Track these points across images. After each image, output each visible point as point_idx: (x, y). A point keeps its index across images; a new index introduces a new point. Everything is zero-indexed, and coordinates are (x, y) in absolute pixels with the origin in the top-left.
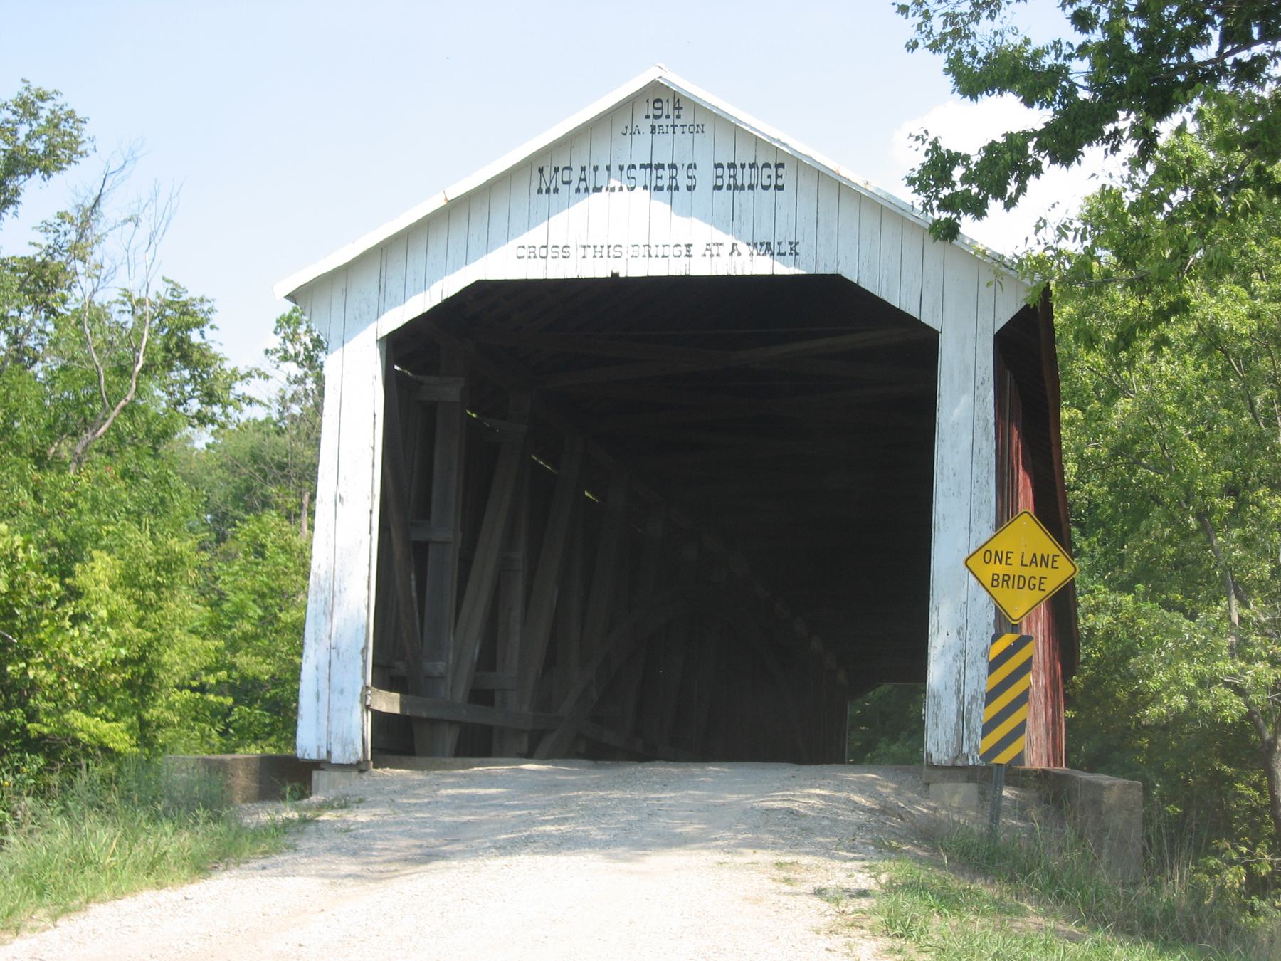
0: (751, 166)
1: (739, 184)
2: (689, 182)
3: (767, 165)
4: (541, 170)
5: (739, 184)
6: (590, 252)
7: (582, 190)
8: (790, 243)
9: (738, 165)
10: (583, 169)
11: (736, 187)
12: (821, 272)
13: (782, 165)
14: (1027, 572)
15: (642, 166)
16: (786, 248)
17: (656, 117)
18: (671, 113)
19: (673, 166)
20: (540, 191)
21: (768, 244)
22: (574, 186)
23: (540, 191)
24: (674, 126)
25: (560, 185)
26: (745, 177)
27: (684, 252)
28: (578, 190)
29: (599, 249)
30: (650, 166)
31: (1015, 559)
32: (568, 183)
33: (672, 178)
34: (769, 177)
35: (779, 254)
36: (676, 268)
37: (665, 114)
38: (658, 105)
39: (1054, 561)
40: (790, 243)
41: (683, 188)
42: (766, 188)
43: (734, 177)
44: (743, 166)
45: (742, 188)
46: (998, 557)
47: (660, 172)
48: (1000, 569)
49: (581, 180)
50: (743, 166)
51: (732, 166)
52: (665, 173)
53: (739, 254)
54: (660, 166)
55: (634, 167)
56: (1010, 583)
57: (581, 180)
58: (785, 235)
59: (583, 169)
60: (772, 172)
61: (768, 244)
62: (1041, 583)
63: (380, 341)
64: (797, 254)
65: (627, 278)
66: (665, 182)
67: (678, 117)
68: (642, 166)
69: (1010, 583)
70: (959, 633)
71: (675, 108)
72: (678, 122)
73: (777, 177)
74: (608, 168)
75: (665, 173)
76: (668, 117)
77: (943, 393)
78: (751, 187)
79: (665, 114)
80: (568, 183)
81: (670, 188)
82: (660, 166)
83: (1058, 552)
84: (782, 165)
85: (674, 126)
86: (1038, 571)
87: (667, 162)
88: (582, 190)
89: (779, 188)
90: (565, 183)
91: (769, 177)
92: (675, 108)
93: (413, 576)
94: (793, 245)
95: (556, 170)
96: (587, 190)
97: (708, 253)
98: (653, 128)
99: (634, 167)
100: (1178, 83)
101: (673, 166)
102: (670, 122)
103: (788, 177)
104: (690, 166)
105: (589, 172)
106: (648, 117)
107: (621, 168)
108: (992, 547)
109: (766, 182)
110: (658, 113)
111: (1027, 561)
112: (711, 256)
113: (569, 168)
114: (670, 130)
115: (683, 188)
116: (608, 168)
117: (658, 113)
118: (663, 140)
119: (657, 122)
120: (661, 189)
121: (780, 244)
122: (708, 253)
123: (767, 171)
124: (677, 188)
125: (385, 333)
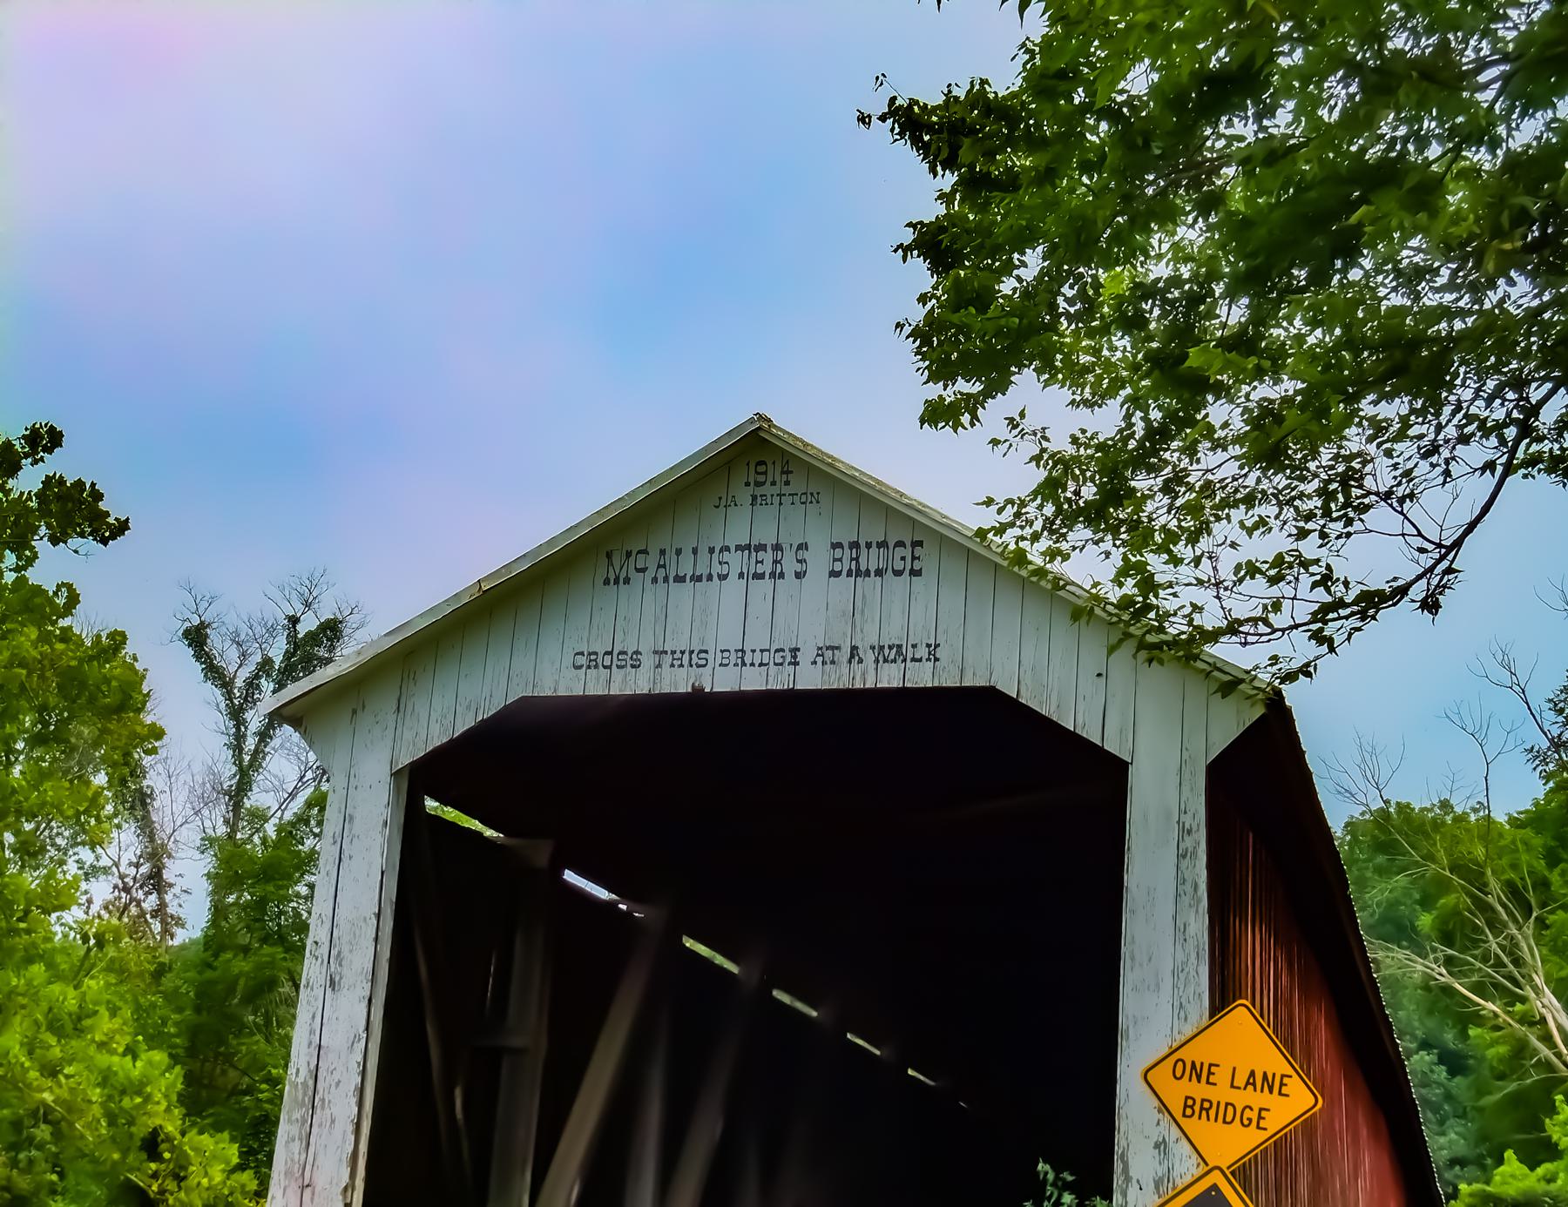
0: (880, 545)
1: (863, 568)
2: (798, 567)
3: (900, 544)
4: (609, 556)
5: (863, 568)
6: (668, 659)
7: (660, 580)
8: (929, 646)
9: (863, 545)
10: (663, 552)
11: (858, 573)
12: (967, 683)
13: (920, 543)
14: (1241, 1098)
15: (738, 548)
16: (922, 652)
17: (758, 484)
18: (777, 479)
19: (777, 547)
20: (607, 582)
21: (900, 647)
22: (650, 574)
23: (607, 582)
24: (780, 495)
25: (633, 574)
26: (871, 560)
27: (789, 659)
28: (655, 580)
29: (678, 655)
30: (748, 547)
31: (1221, 1076)
32: (643, 570)
33: (776, 562)
34: (903, 558)
35: (913, 660)
36: (778, 680)
37: (770, 479)
38: (761, 469)
39: (1282, 1084)
40: (929, 646)
41: (790, 575)
42: (898, 573)
43: (857, 559)
44: (869, 545)
45: (867, 573)
46: (1198, 1072)
47: (761, 555)
48: (1199, 1091)
49: (659, 566)
50: (869, 545)
51: (855, 545)
52: (768, 557)
53: (861, 661)
54: (761, 547)
55: (728, 549)
56: (1212, 1113)
57: (659, 566)
58: (921, 634)
59: (663, 552)
60: (907, 553)
61: (900, 647)
62: (1260, 1118)
63: (396, 775)
64: (936, 659)
65: (711, 693)
66: (767, 568)
67: (787, 483)
68: (738, 548)
69: (1212, 1116)
70: (1157, 1187)
71: (783, 472)
72: (786, 490)
73: (914, 558)
74: (695, 551)
75: (768, 557)
76: (774, 483)
77: (1133, 848)
78: (879, 573)
79: (770, 479)
80: (643, 570)
81: (773, 575)
82: (761, 547)
83: (1290, 1071)
84: (920, 543)
85: (780, 495)
86: (1257, 1099)
87: (770, 540)
88: (660, 580)
89: (915, 573)
90: (638, 570)
91: (903, 558)
92: (783, 472)
93: (458, 1093)
94: (933, 648)
95: (629, 554)
96: (666, 579)
97: (820, 659)
98: (754, 498)
99: (728, 549)
100: (1121, 214)
101: (777, 547)
102: (775, 490)
103: (928, 562)
104: (800, 547)
105: (671, 556)
106: (747, 484)
107: (712, 550)
108: (1187, 1054)
109: (899, 565)
110: (761, 478)
111: (1241, 1080)
112: (824, 663)
113: (645, 552)
114: (776, 500)
115: (790, 575)
116: (695, 551)
117: (761, 478)
118: (766, 513)
119: (759, 491)
120: (760, 576)
121: (914, 646)
122: (820, 659)
123: (900, 552)
124: (782, 575)
125: (405, 760)
